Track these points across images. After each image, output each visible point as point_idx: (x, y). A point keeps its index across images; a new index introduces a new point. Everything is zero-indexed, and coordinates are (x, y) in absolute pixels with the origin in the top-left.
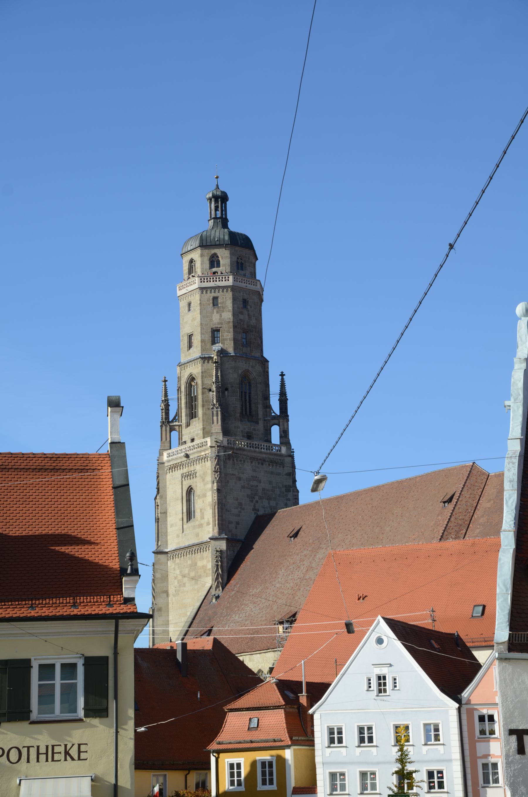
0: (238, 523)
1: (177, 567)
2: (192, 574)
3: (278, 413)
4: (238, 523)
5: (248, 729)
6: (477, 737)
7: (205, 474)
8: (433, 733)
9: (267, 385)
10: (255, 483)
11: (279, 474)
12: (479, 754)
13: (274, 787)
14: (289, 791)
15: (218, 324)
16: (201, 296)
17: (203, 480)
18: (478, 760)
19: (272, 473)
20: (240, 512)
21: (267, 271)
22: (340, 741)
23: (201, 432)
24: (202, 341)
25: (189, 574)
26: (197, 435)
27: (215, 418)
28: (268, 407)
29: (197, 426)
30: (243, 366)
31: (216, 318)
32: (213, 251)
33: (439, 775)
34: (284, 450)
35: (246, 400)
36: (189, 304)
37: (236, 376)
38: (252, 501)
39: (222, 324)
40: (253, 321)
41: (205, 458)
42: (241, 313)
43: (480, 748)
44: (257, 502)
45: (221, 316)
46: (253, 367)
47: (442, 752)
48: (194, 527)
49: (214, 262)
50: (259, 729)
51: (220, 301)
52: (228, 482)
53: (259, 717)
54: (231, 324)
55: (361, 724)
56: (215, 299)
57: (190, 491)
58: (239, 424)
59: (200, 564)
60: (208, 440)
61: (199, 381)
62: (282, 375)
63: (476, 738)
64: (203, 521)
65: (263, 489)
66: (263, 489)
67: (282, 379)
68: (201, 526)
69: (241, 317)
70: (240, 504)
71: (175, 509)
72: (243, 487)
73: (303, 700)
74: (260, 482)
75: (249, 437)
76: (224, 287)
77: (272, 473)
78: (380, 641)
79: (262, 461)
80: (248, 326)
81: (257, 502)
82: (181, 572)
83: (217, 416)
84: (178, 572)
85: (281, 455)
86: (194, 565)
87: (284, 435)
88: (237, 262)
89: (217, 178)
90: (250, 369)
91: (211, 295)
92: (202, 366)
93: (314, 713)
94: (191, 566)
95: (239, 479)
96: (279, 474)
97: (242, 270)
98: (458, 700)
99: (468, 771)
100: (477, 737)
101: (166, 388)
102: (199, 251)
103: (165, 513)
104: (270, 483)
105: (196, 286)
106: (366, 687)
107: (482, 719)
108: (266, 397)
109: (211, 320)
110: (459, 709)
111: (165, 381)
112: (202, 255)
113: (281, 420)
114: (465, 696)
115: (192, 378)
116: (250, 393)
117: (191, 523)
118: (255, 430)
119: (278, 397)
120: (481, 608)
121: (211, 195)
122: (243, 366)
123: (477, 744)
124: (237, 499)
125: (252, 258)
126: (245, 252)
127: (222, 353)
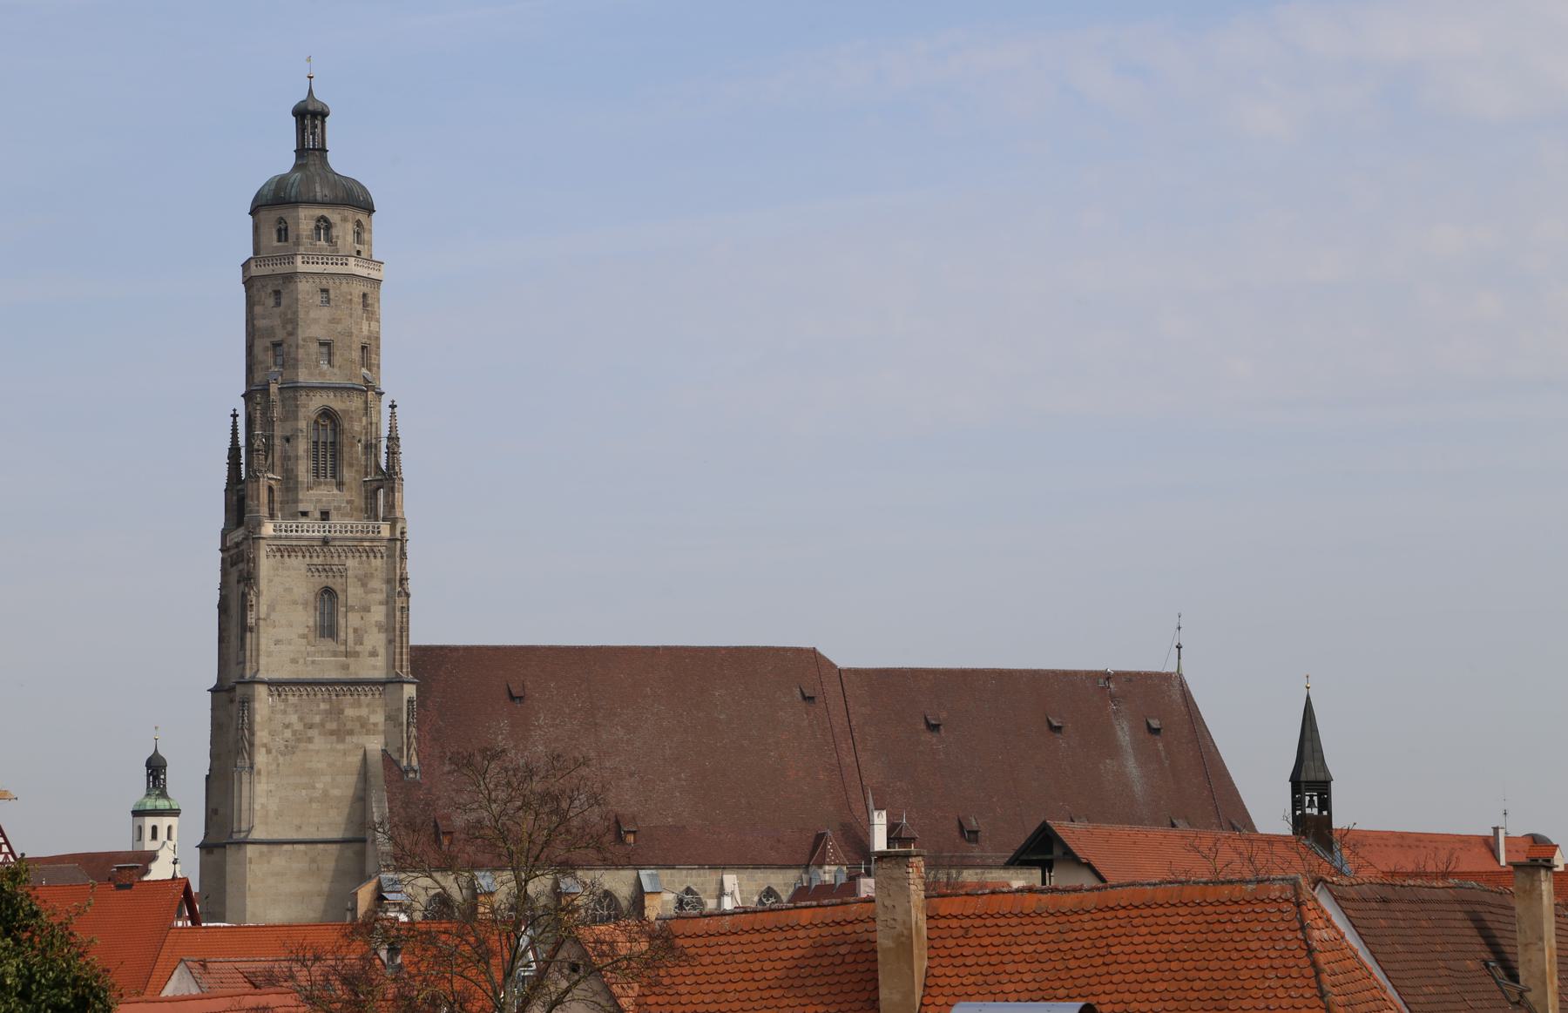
1: (290, 710)
2: (334, 726)
15: (369, 338)
26: (338, 509)
48: (335, 654)
64: (358, 648)
82: (301, 719)
84: (294, 718)
94: (328, 712)
117: (328, 644)
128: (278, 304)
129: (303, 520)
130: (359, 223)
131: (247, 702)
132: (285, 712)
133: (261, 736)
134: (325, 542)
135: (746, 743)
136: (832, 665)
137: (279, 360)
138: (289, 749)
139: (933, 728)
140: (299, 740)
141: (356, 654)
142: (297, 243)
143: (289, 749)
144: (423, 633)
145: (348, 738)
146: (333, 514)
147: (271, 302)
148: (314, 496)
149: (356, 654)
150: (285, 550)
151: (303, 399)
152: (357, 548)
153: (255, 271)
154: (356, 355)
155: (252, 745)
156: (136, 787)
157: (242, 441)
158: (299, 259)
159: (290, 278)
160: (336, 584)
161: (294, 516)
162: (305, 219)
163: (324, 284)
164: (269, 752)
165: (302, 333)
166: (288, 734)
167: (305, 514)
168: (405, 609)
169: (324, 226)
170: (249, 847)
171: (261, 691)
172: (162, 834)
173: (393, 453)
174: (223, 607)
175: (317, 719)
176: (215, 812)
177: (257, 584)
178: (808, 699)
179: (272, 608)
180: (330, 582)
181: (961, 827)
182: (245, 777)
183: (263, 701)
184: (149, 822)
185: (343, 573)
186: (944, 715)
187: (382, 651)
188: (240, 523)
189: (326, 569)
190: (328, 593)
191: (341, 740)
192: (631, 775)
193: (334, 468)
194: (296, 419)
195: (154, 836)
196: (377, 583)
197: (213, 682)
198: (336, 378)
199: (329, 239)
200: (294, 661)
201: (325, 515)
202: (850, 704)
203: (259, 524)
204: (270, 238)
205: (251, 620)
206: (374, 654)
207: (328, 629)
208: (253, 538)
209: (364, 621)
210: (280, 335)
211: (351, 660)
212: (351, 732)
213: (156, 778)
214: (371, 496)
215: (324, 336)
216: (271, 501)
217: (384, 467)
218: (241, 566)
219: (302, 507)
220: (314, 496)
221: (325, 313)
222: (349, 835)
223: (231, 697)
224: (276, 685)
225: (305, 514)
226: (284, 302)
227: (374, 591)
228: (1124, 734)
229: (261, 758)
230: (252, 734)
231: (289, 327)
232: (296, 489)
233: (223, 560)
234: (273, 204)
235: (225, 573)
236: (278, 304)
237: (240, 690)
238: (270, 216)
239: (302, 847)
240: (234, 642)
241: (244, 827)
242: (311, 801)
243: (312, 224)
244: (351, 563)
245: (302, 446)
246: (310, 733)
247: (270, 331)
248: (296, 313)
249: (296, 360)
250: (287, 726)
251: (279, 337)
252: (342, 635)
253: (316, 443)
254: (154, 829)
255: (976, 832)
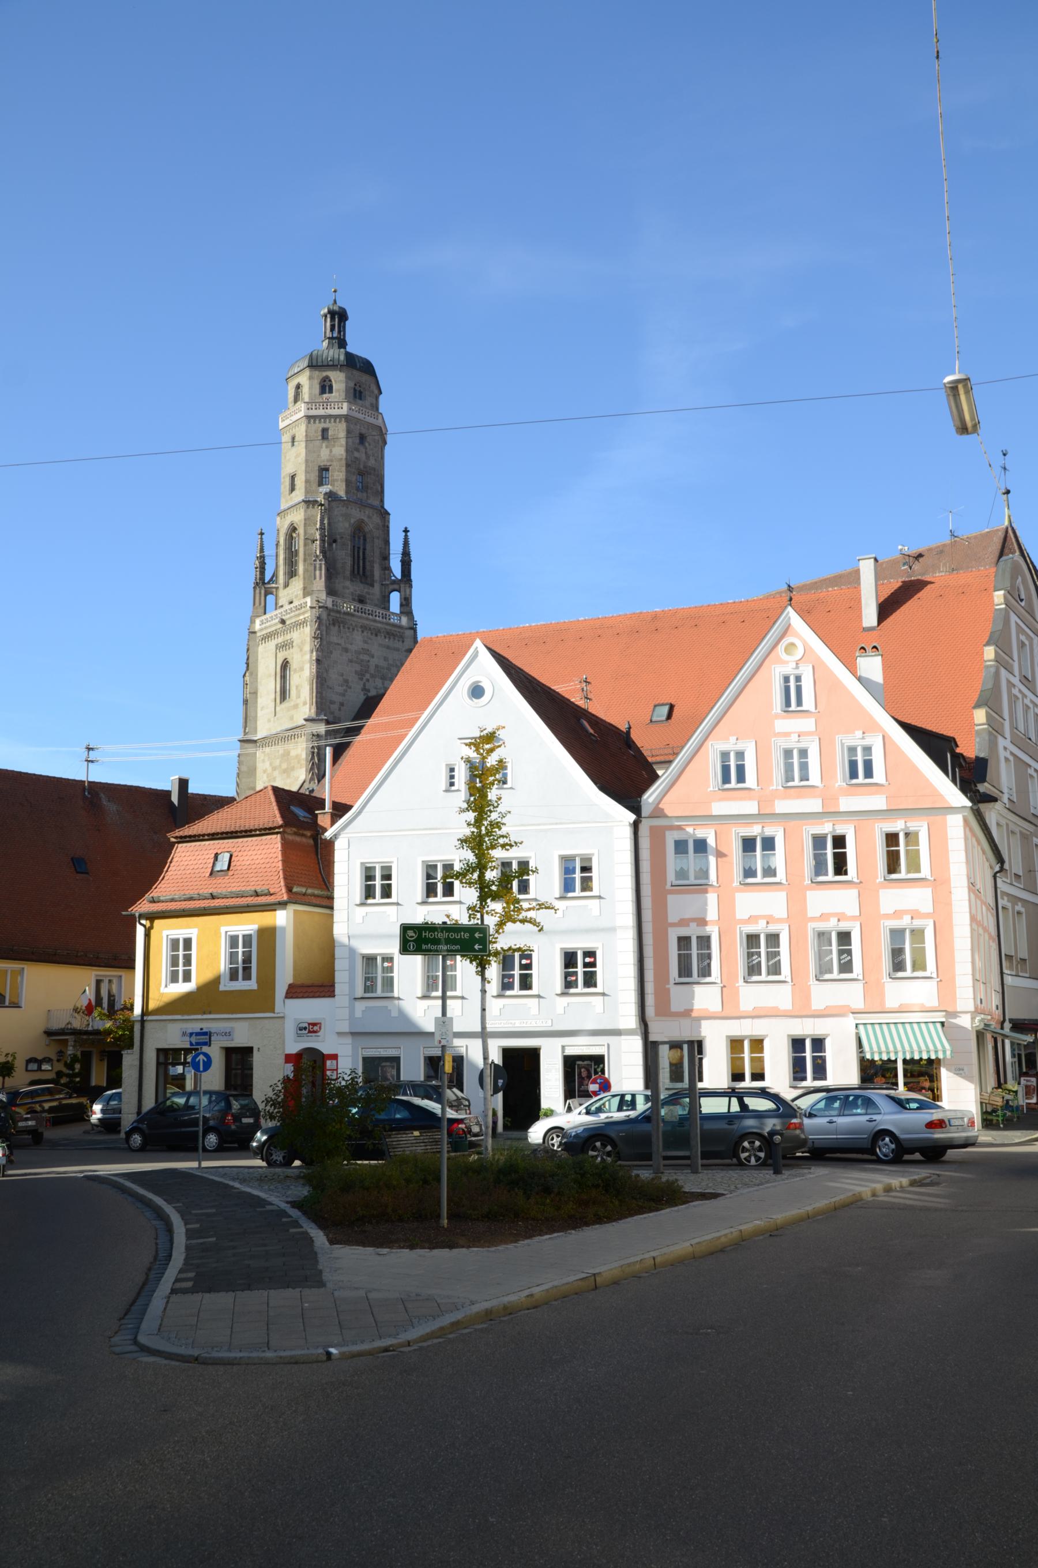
0: (342, 704)
2: (284, 766)
3: (399, 577)
4: (342, 704)
5: (211, 874)
6: (669, 884)
7: (303, 643)
8: (578, 875)
9: (387, 542)
10: (366, 658)
11: (398, 650)
12: (672, 918)
13: (252, 985)
14: (281, 989)
15: (328, 461)
16: (307, 427)
17: (301, 650)
18: (670, 930)
19: (388, 647)
20: (346, 691)
21: (392, 407)
22: (387, 892)
23: (301, 593)
24: (307, 481)
26: (296, 596)
27: (318, 572)
28: (387, 569)
29: (297, 585)
30: (356, 514)
31: (324, 454)
32: (325, 374)
33: (588, 960)
34: (404, 621)
35: (359, 557)
36: (293, 438)
37: (347, 525)
38: (361, 679)
39: (332, 461)
40: (372, 462)
41: (304, 623)
42: (357, 450)
43: (678, 906)
44: (368, 680)
45: (331, 451)
46: (369, 517)
47: (596, 912)
49: (326, 387)
50: (230, 873)
51: (330, 433)
52: (331, 653)
53: (233, 850)
54: (344, 462)
55: (432, 858)
56: (325, 431)
57: (285, 665)
58: (348, 583)
59: (293, 753)
60: (308, 599)
61: (301, 530)
62: (406, 531)
63: (668, 887)
64: (298, 701)
65: (377, 666)
66: (377, 666)
67: (406, 536)
68: (296, 706)
69: (356, 454)
70: (346, 681)
71: (267, 686)
72: (351, 661)
73: (323, 820)
74: (373, 657)
75: (361, 600)
76: (336, 417)
77: (388, 647)
78: (477, 692)
79: (377, 633)
80: (365, 467)
81: (368, 680)
82: (271, 764)
83: (320, 570)
84: (267, 765)
85: (400, 627)
86: (287, 754)
87: (406, 603)
88: (355, 390)
89: (335, 291)
90: (366, 519)
91: (319, 426)
92: (305, 511)
93: (336, 836)
94: (283, 755)
95: (346, 650)
96: (398, 650)
97: (361, 399)
98: (635, 808)
99: (649, 951)
100: (669, 884)
101: (262, 541)
102: (307, 373)
103: (255, 693)
104: (386, 659)
105: (302, 414)
106: (443, 783)
107: (681, 847)
108: (386, 557)
109: (319, 456)
110: (636, 825)
111: (262, 534)
112: (311, 378)
113: (402, 586)
114: (651, 800)
115: (293, 529)
116: (364, 549)
117: (285, 704)
118: (368, 593)
119: (399, 557)
120: (666, 709)
121: (326, 310)
122: (356, 514)
123: (671, 898)
124: (342, 675)
125: (374, 387)
126: (365, 378)
127: (331, 496)
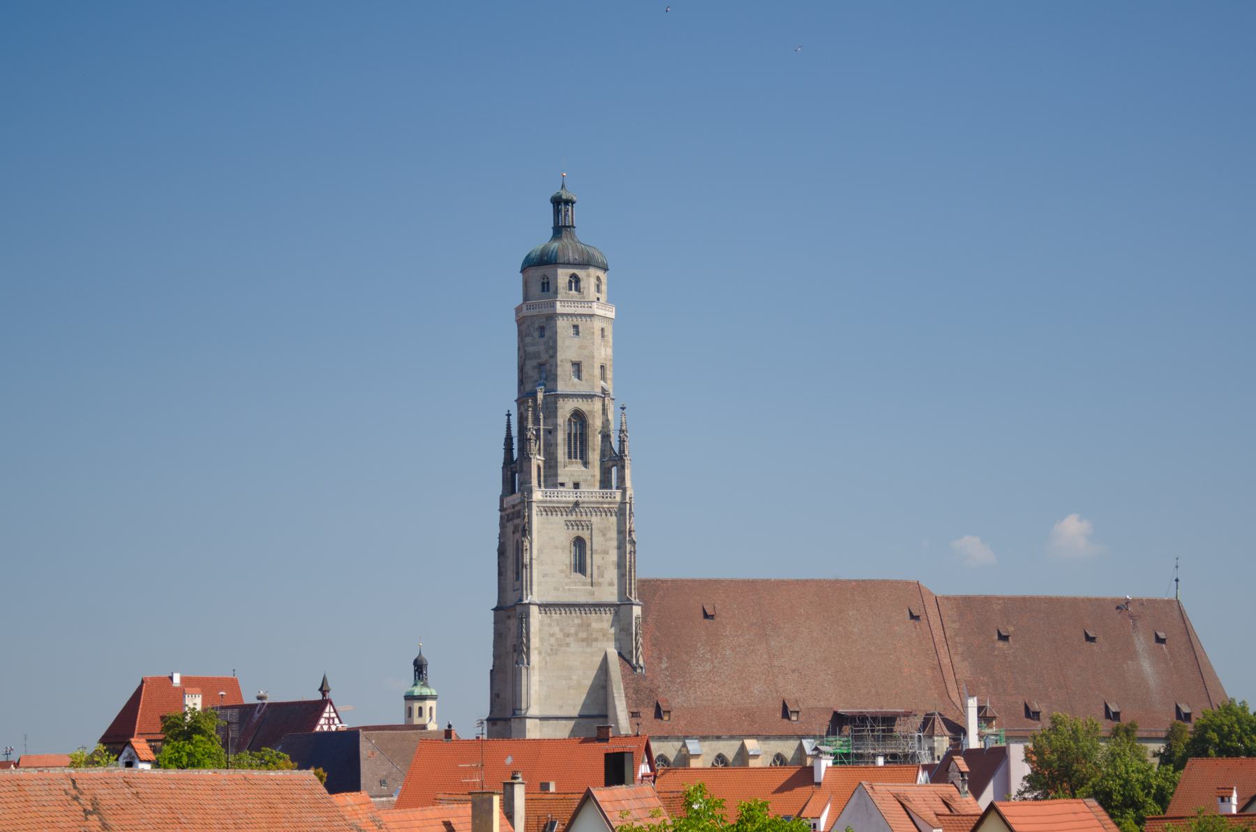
2: (583, 635)
25: (576, 634)
26: (586, 481)
48: (584, 584)
59: (595, 625)
64: (600, 580)
82: (561, 630)
84: (556, 629)
86: (586, 626)
94: (581, 626)
128: (542, 336)
129: (560, 489)
130: (598, 278)
131: (524, 617)
132: (550, 625)
133: (535, 642)
134: (577, 504)
135: (873, 649)
136: (930, 593)
137: (544, 375)
138: (554, 652)
139: (1003, 638)
140: (560, 645)
141: (600, 584)
142: (556, 293)
143: (554, 652)
144: (645, 569)
145: (594, 644)
146: (582, 485)
147: (536, 334)
148: (569, 470)
149: (600, 584)
150: (549, 510)
151: (560, 403)
152: (597, 510)
153: (525, 312)
154: (597, 371)
155: (528, 648)
156: (406, 682)
157: (515, 433)
158: (558, 304)
159: (552, 317)
160: (585, 534)
161: (555, 486)
162: (563, 275)
163: (575, 323)
164: (540, 653)
165: (560, 356)
166: (553, 640)
167: (562, 485)
168: (633, 552)
169: (575, 281)
170: (528, 721)
171: (534, 610)
172: (426, 712)
173: (622, 442)
174: (502, 552)
175: (573, 630)
176: (498, 696)
177: (530, 534)
178: (912, 617)
179: (540, 551)
180: (580, 533)
181: (1027, 708)
182: (524, 671)
183: (536, 618)
184: (416, 705)
185: (589, 527)
186: (1011, 629)
187: (616, 581)
188: (513, 492)
189: (578, 524)
190: (579, 543)
191: (589, 645)
192: (793, 671)
193: (581, 451)
194: (556, 417)
195: (420, 714)
196: (613, 534)
197: (495, 605)
198: (582, 387)
199: (578, 289)
200: (556, 589)
201: (576, 486)
202: (945, 619)
203: (530, 491)
204: (536, 289)
205: (526, 559)
206: (611, 584)
207: (580, 567)
208: (527, 503)
209: (604, 558)
210: (544, 357)
211: (595, 588)
212: (596, 640)
213: (421, 672)
214: (605, 473)
215: (576, 359)
216: (539, 476)
217: (617, 451)
218: (517, 521)
219: (560, 480)
220: (569, 470)
221: (576, 339)
222: (595, 712)
223: (510, 617)
224: (544, 607)
225: (562, 485)
226: (547, 333)
227: (611, 539)
228: (1141, 642)
229: (535, 658)
230: (528, 640)
231: (551, 352)
232: (556, 467)
233: (501, 517)
234: (540, 265)
235: (502, 526)
236: (542, 336)
237: (519, 609)
238: (537, 273)
239: (564, 722)
240: (510, 574)
241: (524, 706)
242: (569, 688)
243: (567, 279)
244: (595, 520)
245: (561, 436)
246: (568, 640)
247: (537, 355)
248: (555, 342)
249: (556, 375)
250: (552, 635)
251: (542, 360)
252: (589, 570)
253: (569, 435)
254: (420, 709)
255: (1038, 713)
